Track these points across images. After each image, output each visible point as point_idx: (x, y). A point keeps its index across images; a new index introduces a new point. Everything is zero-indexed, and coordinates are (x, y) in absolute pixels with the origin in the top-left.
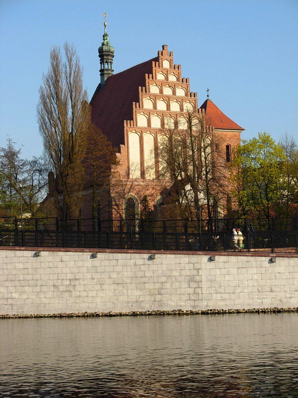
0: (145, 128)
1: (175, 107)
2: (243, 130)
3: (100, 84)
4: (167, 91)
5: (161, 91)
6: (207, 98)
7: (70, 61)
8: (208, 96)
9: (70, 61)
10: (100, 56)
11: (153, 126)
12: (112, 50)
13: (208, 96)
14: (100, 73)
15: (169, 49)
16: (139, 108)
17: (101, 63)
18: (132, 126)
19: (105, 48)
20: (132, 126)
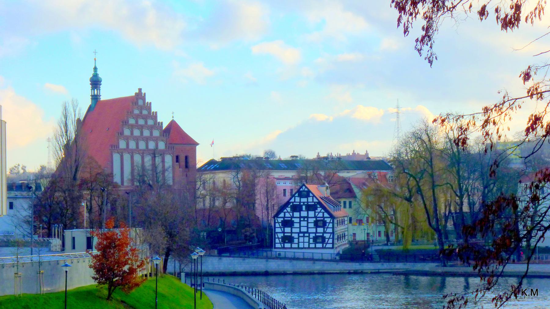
0: (124, 149)
1: (146, 133)
2: (198, 144)
3: (90, 106)
4: (141, 122)
5: (137, 122)
7: (75, 111)
8: (173, 117)
9: (75, 111)
10: (91, 84)
11: (130, 147)
12: (100, 80)
13: (173, 117)
14: (91, 97)
15: (143, 92)
16: (121, 135)
17: (92, 90)
18: (115, 148)
19: (95, 79)
20: (115, 148)
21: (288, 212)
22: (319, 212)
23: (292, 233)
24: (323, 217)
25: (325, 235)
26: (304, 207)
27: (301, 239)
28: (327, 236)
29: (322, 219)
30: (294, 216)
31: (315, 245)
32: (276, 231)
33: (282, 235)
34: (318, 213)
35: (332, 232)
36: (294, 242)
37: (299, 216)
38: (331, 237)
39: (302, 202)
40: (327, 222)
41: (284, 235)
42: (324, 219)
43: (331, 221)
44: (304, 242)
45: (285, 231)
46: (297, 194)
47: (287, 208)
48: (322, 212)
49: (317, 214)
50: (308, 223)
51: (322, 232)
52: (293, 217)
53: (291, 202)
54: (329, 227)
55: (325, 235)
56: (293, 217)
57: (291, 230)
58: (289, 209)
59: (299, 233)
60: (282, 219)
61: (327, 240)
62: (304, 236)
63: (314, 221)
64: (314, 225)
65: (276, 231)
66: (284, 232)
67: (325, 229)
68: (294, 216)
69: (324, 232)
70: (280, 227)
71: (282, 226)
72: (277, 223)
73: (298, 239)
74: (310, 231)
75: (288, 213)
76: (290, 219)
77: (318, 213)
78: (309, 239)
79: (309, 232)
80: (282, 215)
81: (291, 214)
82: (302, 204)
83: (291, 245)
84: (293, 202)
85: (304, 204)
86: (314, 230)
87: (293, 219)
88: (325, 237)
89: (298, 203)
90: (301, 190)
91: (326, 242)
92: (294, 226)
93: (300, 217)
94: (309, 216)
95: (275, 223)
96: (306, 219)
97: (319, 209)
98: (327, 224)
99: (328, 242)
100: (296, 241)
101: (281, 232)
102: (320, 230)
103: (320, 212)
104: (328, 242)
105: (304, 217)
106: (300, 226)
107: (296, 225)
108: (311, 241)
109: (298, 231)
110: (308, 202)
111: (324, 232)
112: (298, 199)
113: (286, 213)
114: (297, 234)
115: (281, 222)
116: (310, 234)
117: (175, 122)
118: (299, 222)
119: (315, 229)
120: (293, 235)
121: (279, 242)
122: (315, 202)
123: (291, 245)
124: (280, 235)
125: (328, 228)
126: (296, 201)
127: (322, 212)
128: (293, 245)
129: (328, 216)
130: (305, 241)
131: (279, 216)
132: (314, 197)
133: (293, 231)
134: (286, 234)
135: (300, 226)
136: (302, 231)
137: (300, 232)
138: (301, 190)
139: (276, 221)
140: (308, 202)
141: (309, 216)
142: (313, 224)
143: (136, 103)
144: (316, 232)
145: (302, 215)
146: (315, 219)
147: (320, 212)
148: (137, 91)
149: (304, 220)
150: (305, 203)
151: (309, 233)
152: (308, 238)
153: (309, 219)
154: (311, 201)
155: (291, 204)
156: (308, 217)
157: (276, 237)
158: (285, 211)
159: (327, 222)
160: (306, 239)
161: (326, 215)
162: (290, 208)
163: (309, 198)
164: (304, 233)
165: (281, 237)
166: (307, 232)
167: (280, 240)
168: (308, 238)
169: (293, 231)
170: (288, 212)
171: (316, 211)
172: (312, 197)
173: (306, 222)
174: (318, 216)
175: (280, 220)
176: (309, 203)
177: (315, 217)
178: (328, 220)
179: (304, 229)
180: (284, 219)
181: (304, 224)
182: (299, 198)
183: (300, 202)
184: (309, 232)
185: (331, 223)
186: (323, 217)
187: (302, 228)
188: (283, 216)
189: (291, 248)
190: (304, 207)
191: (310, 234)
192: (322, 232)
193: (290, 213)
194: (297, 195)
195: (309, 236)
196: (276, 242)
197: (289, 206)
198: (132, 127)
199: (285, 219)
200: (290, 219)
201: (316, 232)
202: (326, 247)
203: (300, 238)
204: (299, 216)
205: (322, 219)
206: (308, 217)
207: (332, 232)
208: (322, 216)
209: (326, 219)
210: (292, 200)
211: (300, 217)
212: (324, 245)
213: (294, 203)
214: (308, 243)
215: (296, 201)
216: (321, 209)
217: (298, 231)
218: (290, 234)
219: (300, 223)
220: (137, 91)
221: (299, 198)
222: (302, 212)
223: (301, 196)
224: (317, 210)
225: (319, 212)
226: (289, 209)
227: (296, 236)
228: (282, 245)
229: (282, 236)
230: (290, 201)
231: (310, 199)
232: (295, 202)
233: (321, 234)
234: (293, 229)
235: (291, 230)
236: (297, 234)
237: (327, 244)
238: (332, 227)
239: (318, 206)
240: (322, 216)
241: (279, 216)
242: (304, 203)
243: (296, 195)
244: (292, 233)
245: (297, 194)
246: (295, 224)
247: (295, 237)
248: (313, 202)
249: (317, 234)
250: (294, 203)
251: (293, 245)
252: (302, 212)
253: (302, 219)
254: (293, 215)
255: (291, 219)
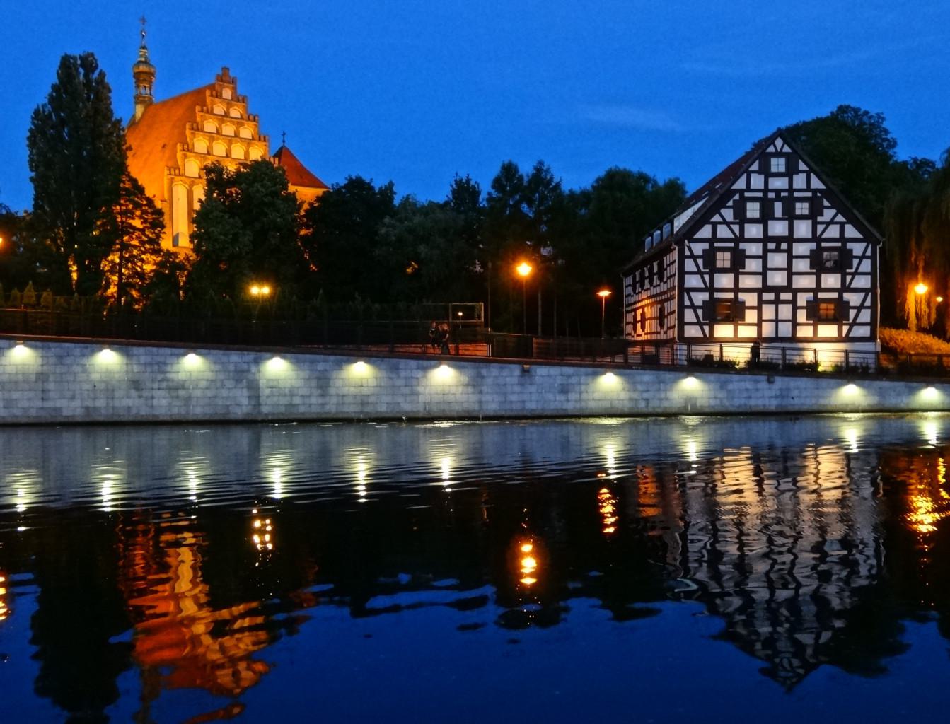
4: (228, 129)
6: (281, 144)
15: (232, 74)
19: (143, 68)
21: (725, 222)
22: (828, 224)
23: (736, 289)
24: (842, 239)
25: (846, 296)
26: (778, 208)
27: (768, 312)
28: (853, 299)
29: (839, 244)
30: (747, 235)
31: (815, 331)
32: (687, 285)
33: (705, 296)
34: (824, 226)
35: (869, 286)
36: (743, 318)
37: (761, 236)
38: (868, 303)
39: (772, 191)
40: (854, 254)
41: (711, 296)
42: (844, 245)
43: (869, 253)
44: (777, 321)
45: (716, 286)
46: (757, 162)
47: (723, 211)
48: (837, 223)
49: (820, 228)
50: (791, 258)
51: (838, 285)
52: (741, 238)
53: (736, 191)
54: (860, 271)
55: (846, 296)
56: (741, 238)
57: (736, 281)
58: (728, 214)
59: (759, 292)
60: (706, 246)
61: (852, 313)
62: (777, 302)
63: (811, 251)
64: (811, 268)
65: (687, 285)
66: (711, 289)
67: (849, 278)
68: (747, 235)
69: (845, 288)
70: (699, 273)
71: (704, 268)
72: (688, 257)
73: (759, 308)
74: (800, 282)
75: (725, 226)
76: (732, 245)
77: (824, 226)
78: (795, 309)
79: (794, 286)
80: (706, 232)
81: (736, 228)
82: (772, 195)
83: (736, 331)
84: (741, 192)
85: (778, 198)
86: (809, 282)
87: (742, 246)
88: (848, 303)
89: (760, 195)
90: (771, 149)
91: (851, 321)
92: (744, 269)
93: (766, 239)
94: (795, 237)
95: (682, 258)
96: (784, 246)
97: (828, 214)
98: (855, 262)
99: (858, 321)
100: (751, 316)
101: (703, 286)
102: (832, 280)
103: (832, 222)
104: (858, 321)
105: (778, 240)
106: (765, 269)
107: (753, 265)
108: (802, 316)
109: (760, 286)
110: (791, 190)
111: (845, 288)
112: (757, 181)
113: (719, 227)
114: (755, 295)
115: (701, 253)
116: (799, 295)
117: (287, 149)
118: (760, 253)
119: (814, 277)
120: (742, 296)
121: (695, 321)
122: (815, 191)
123: (736, 331)
124: (700, 298)
125: (854, 275)
126: (752, 187)
127: (837, 223)
128: (740, 327)
129: (860, 236)
130: (779, 318)
131: (697, 236)
132: (813, 176)
133: (741, 286)
134: (717, 295)
135: (763, 275)
136: (770, 283)
137: (766, 288)
138: (771, 149)
139: (687, 253)
140: (791, 190)
141: (795, 237)
142: (808, 261)
143: (219, 96)
144: (818, 288)
145: (770, 233)
146: (813, 245)
147: (832, 222)
148: (220, 73)
149: (778, 250)
150: (783, 194)
151: (795, 292)
152: (790, 306)
153: (795, 245)
154: (805, 187)
155: (737, 197)
156: (790, 239)
157: (687, 303)
158: (716, 218)
159: (854, 254)
160: (785, 311)
161: (851, 232)
162: (731, 211)
163: (795, 177)
164: (777, 290)
165: (701, 304)
166: (788, 288)
167: (700, 312)
168: (790, 306)
169: (741, 286)
170: (725, 222)
171: (820, 219)
172: (805, 175)
173: (785, 255)
174: (824, 236)
175: (698, 249)
176: (796, 194)
177: (816, 238)
178: (858, 248)
179: (778, 279)
180: (711, 245)
181: (778, 260)
182: (762, 177)
183: (766, 190)
184: (794, 286)
185: (868, 258)
186: (842, 239)
187: (769, 273)
188: (710, 236)
189: (736, 340)
190: (778, 208)
191: (799, 295)
192: (838, 285)
193: (732, 226)
194: (755, 167)
195: (794, 302)
196: (686, 320)
197: (730, 203)
198: (212, 138)
199: (716, 245)
200: (732, 245)
201: (818, 288)
202: (851, 335)
203: (764, 306)
204: (761, 236)
205: (839, 244)
206: (790, 239)
207: (869, 286)
208: (837, 235)
209: (849, 245)
210: (741, 184)
211: (766, 239)
212: (845, 329)
213: (747, 194)
214: (790, 323)
215: (752, 187)
216: (834, 211)
217: (760, 286)
218: (730, 295)
219: (764, 258)
220: (220, 73)
221: (762, 177)
222: (770, 222)
223: (766, 172)
224: (822, 214)
225: (828, 224)
226: (728, 214)
227: (750, 299)
228: (706, 328)
229: (704, 302)
230: (734, 187)
231: (799, 181)
232: (748, 189)
233: (835, 295)
234: (741, 277)
235: (736, 281)
236: (755, 295)
237: (855, 328)
238: (868, 269)
239: (826, 203)
240: (837, 235)
241: (697, 236)
242: (778, 192)
243: (752, 168)
244: (736, 289)
245: (757, 162)
246: (747, 261)
247: (747, 305)
248: (808, 189)
249: (821, 295)
250: (747, 194)
251: (741, 328)
252: (770, 222)
253: (772, 246)
254: (742, 230)
255: (737, 245)
